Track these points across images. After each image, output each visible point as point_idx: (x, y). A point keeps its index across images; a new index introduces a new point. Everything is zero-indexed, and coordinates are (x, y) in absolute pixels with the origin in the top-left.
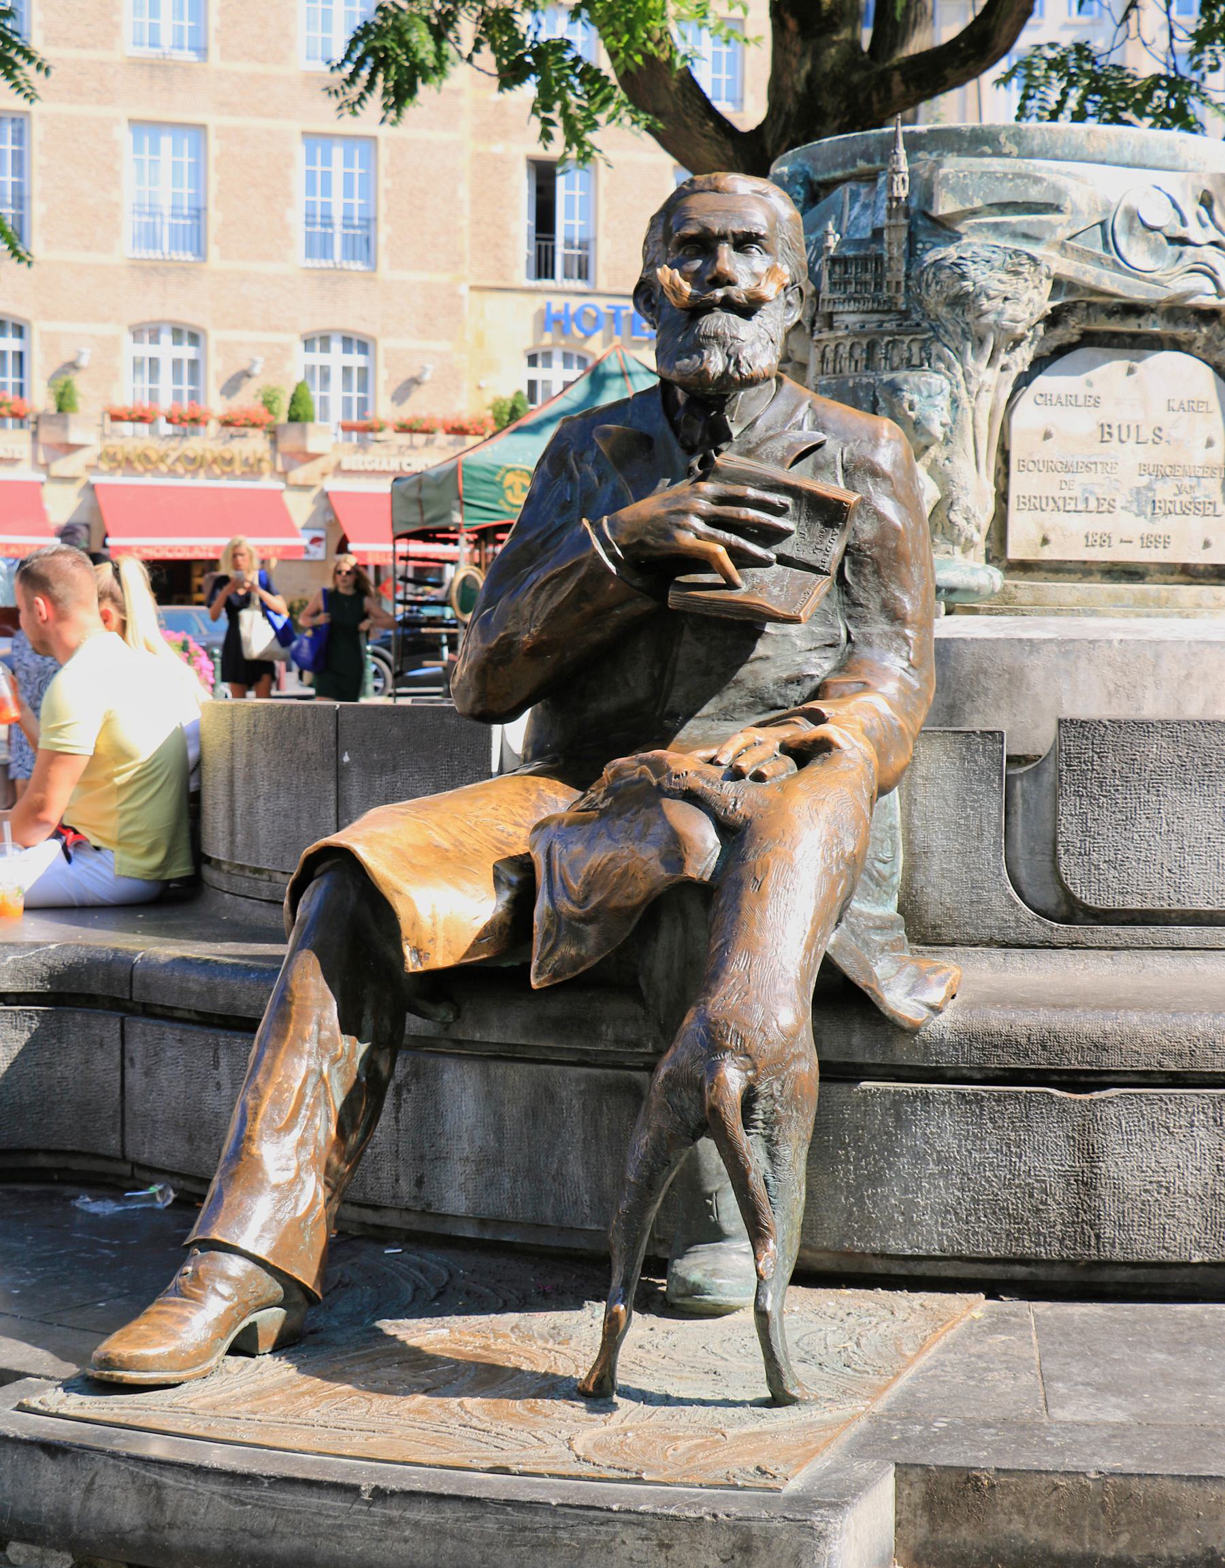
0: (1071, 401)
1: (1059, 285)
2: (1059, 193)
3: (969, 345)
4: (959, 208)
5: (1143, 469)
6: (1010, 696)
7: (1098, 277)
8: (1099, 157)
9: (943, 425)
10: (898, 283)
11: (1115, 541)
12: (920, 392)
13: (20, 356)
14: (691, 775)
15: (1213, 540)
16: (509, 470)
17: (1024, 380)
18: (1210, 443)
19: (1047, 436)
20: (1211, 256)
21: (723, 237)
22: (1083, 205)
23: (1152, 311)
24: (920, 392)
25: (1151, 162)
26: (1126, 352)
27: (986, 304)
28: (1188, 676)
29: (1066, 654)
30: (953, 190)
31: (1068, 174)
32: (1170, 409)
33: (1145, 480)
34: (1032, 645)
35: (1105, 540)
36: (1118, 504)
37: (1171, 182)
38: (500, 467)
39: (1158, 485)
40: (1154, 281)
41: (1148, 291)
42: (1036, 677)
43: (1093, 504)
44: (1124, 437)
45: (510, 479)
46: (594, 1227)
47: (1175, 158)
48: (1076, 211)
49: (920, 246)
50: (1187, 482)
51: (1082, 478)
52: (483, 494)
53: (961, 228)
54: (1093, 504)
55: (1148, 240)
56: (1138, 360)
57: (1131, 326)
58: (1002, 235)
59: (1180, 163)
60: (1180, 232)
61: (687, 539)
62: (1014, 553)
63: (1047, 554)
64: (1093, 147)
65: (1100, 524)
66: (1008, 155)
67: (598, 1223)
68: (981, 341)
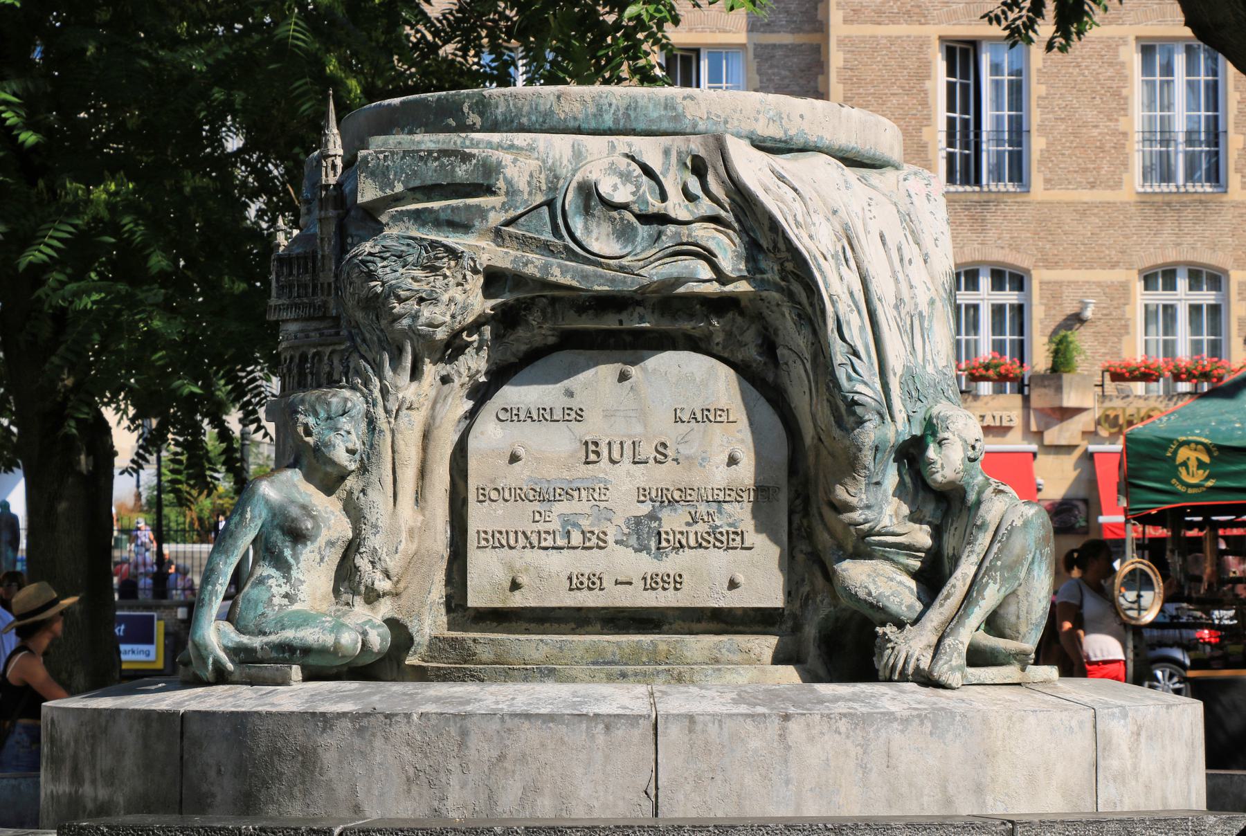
1: (494, 280)
3: (386, 357)
4: (380, 194)
5: (643, 494)
6: (303, 783)
7: (546, 267)
8: (572, 124)
9: (352, 452)
10: (329, 284)
12: (316, 414)
13: (1020, 308)
15: (740, 578)
16: (1186, 443)
17: (480, 394)
22: (522, 184)
23: (639, 303)
24: (316, 414)
25: (641, 126)
26: (617, 353)
27: (398, 308)
28: (502, 758)
29: (361, 731)
30: (372, 174)
32: (678, 420)
33: (645, 509)
34: (325, 721)
35: (594, 582)
36: (610, 539)
37: (650, 150)
38: (1171, 441)
39: (665, 514)
40: (622, 269)
41: (613, 281)
42: (329, 758)
43: (576, 538)
44: (616, 456)
45: (1183, 454)
47: (676, 118)
48: (512, 192)
49: (349, 240)
50: (702, 508)
51: (561, 508)
52: (1151, 473)
53: (384, 219)
54: (576, 538)
55: (612, 220)
56: (633, 363)
57: (610, 322)
58: (424, 224)
59: (686, 125)
60: (655, 206)
63: (517, 600)
64: (564, 111)
65: (587, 562)
66: (472, 129)
68: (400, 350)
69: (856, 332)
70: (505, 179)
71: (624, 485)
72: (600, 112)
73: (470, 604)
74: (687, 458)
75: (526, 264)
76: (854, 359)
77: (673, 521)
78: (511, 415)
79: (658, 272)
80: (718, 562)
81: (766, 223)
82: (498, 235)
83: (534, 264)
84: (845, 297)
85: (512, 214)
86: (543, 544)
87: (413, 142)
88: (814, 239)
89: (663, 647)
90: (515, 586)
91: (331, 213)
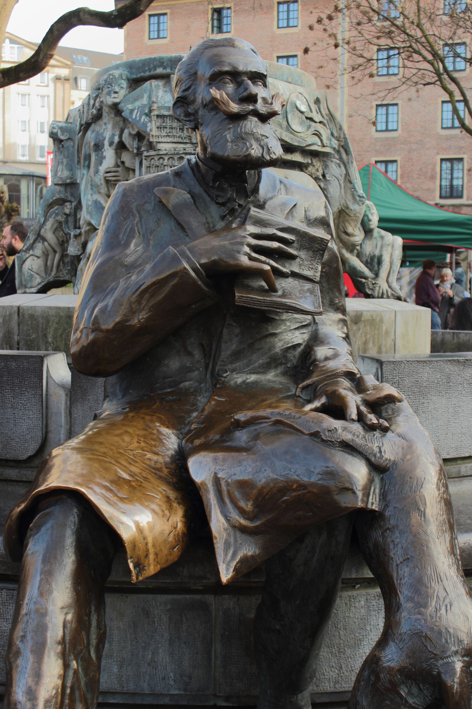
14: (340, 431)
20: (320, 128)
21: (245, 73)
41: (299, 142)
46: (177, 692)
61: (245, 261)
67: (179, 690)
81: (338, 127)
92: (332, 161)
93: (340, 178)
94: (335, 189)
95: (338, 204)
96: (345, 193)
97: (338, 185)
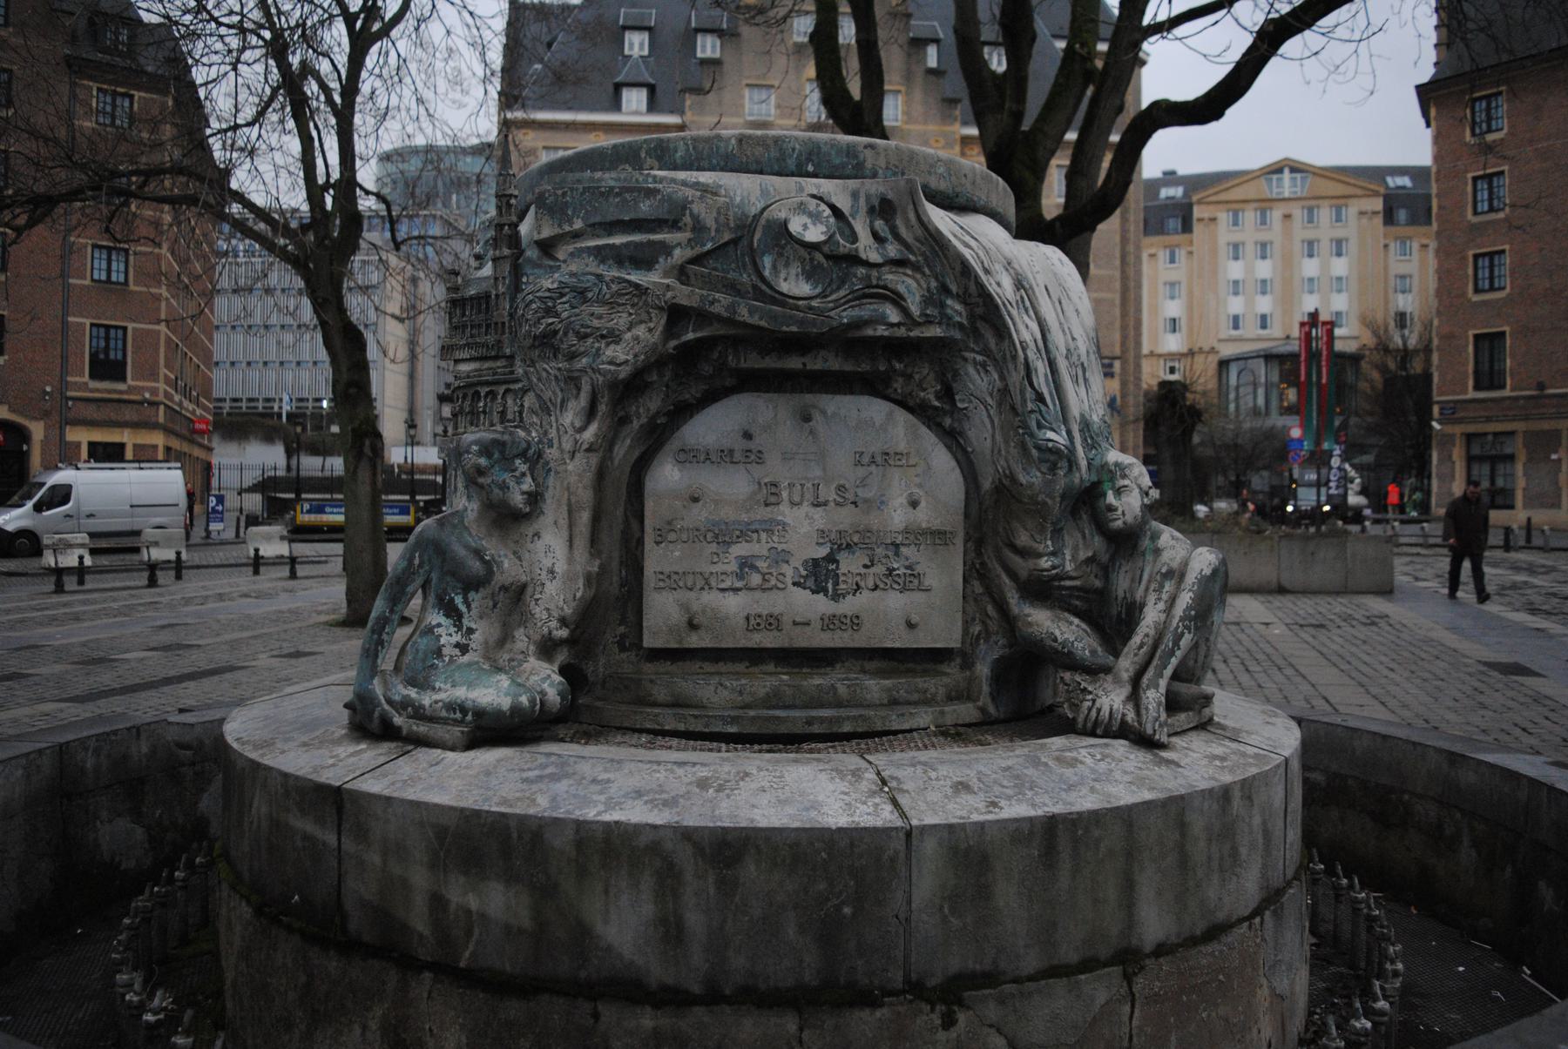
0: (726, 456)
2: (684, 206)
4: (558, 231)
7: (732, 308)
11: (787, 626)
18: (914, 504)
19: (696, 500)
22: (710, 222)
31: (684, 183)
33: (822, 552)
37: (835, 190)
39: (842, 557)
41: (802, 322)
48: (699, 228)
50: (880, 551)
54: (756, 579)
57: (794, 363)
58: (603, 261)
60: (844, 246)
62: (648, 642)
69: (1042, 379)
70: (691, 214)
71: (803, 529)
72: (782, 157)
73: (645, 644)
74: (866, 501)
75: (712, 303)
76: (1043, 408)
77: (849, 564)
78: (688, 456)
79: (847, 315)
80: (895, 602)
81: (958, 268)
82: (682, 273)
83: (721, 302)
84: (1032, 345)
85: (698, 250)
86: (723, 586)
87: (592, 179)
88: (1002, 287)
89: (842, 690)
90: (692, 626)
91: (506, 252)
92: (966, 360)
93: (989, 400)
94: (982, 431)
95: (991, 470)
96: (1006, 442)
97: (987, 421)
